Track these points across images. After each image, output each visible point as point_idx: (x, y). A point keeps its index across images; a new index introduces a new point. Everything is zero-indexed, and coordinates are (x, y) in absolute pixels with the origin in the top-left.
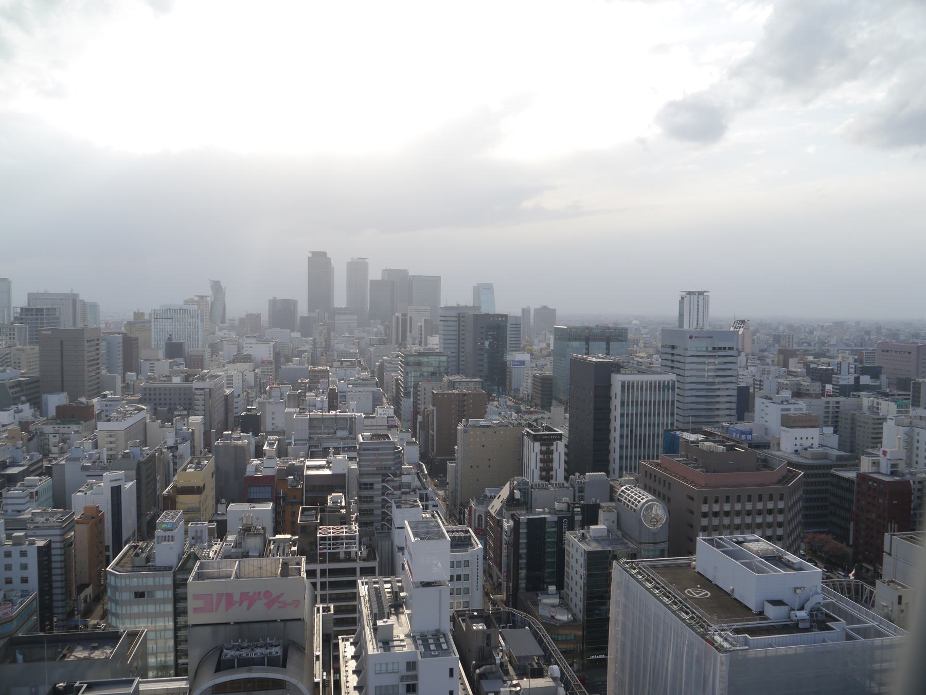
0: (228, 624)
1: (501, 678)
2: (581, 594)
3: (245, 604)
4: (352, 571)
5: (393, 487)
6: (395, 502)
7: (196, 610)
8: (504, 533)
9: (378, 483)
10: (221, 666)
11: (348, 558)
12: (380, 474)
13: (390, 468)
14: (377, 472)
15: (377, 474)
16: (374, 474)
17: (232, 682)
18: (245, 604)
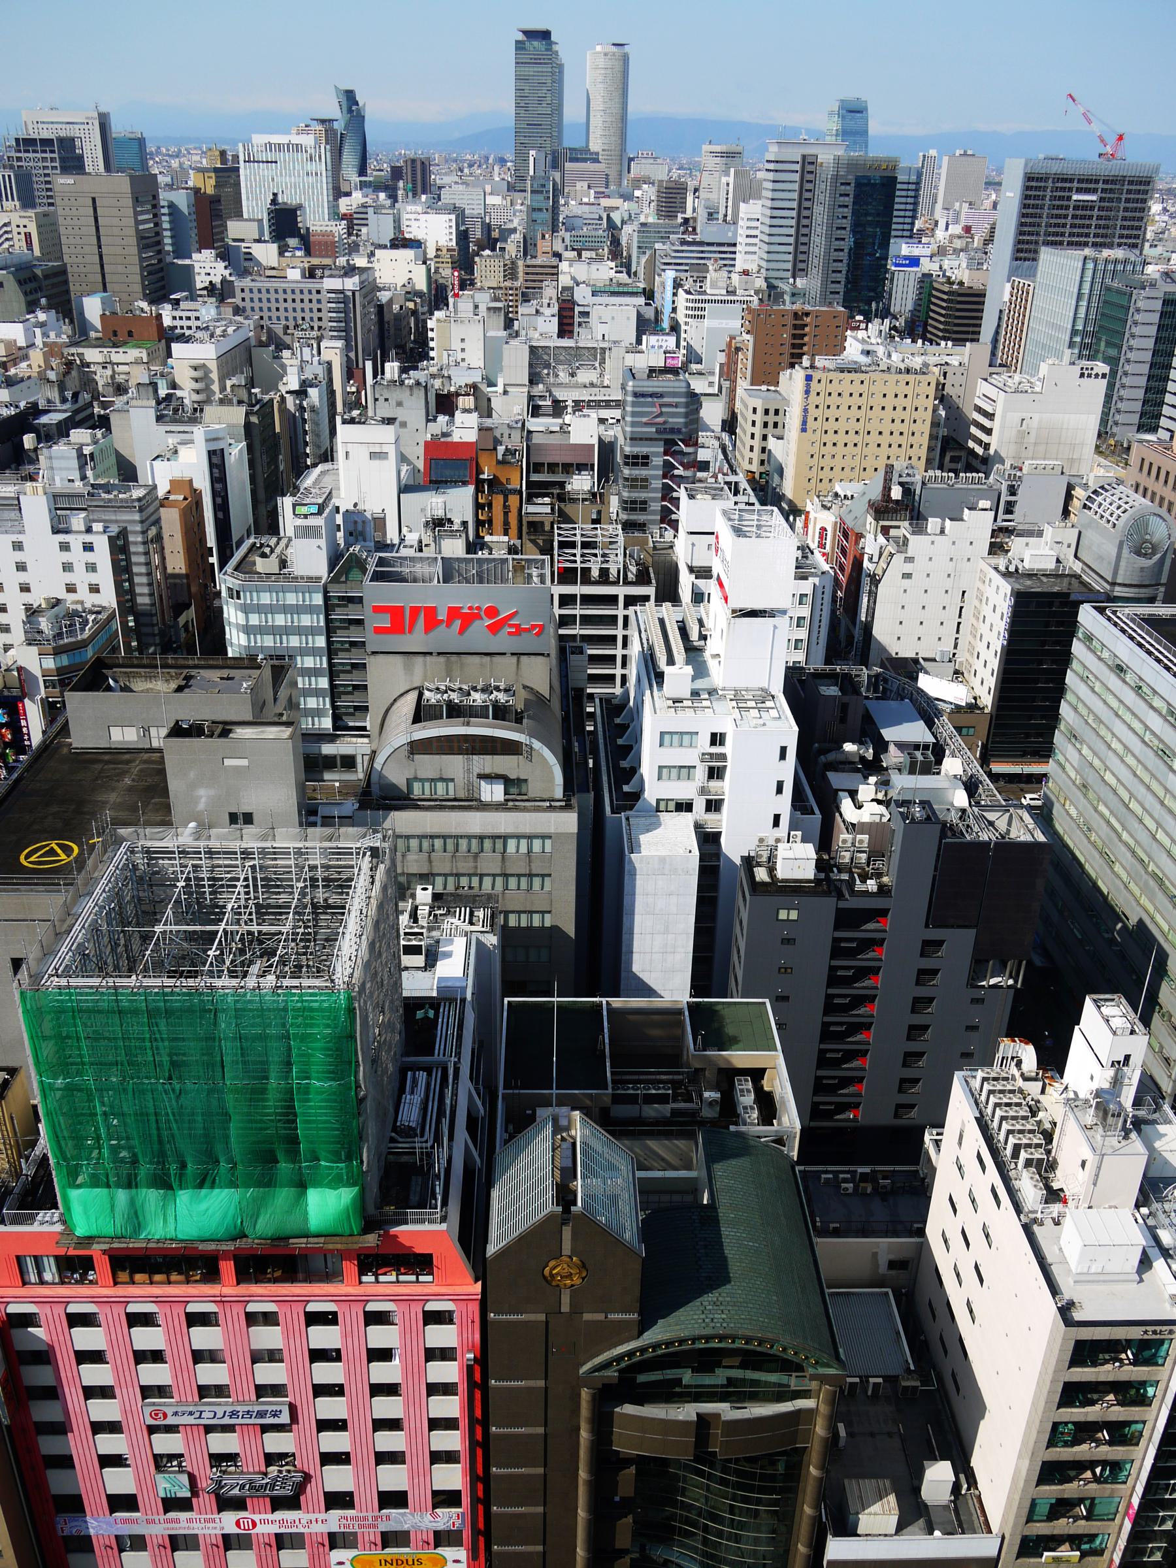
0: (431, 654)
1: (858, 770)
2: (994, 663)
3: (457, 623)
4: (612, 600)
5: (682, 464)
6: (686, 489)
7: (378, 630)
8: (866, 557)
9: (656, 454)
10: (421, 714)
11: (604, 578)
12: (660, 440)
13: (679, 431)
14: (657, 436)
15: (656, 439)
16: (651, 439)
17: (439, 738)
18: (457, 623)
